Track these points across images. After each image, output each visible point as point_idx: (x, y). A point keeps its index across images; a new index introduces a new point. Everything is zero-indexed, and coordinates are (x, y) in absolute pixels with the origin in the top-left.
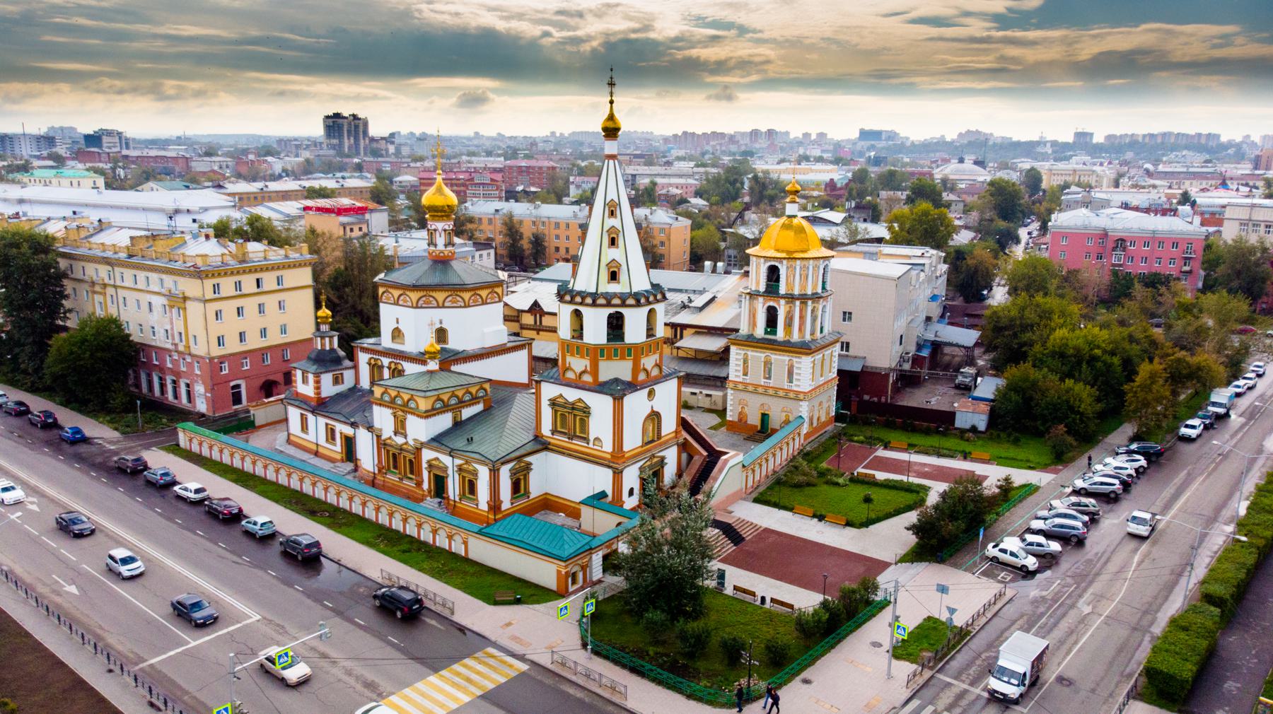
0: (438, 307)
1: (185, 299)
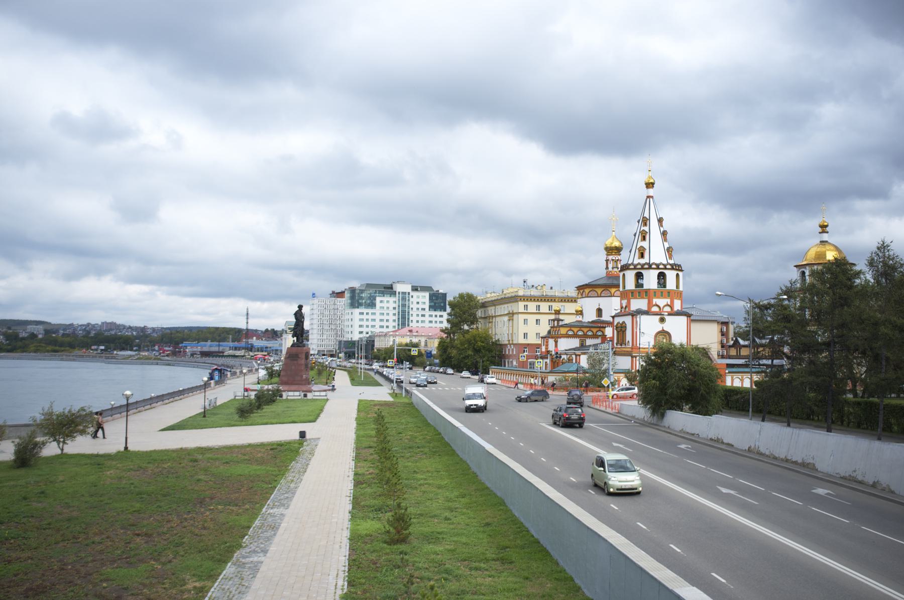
1: (513, 314)
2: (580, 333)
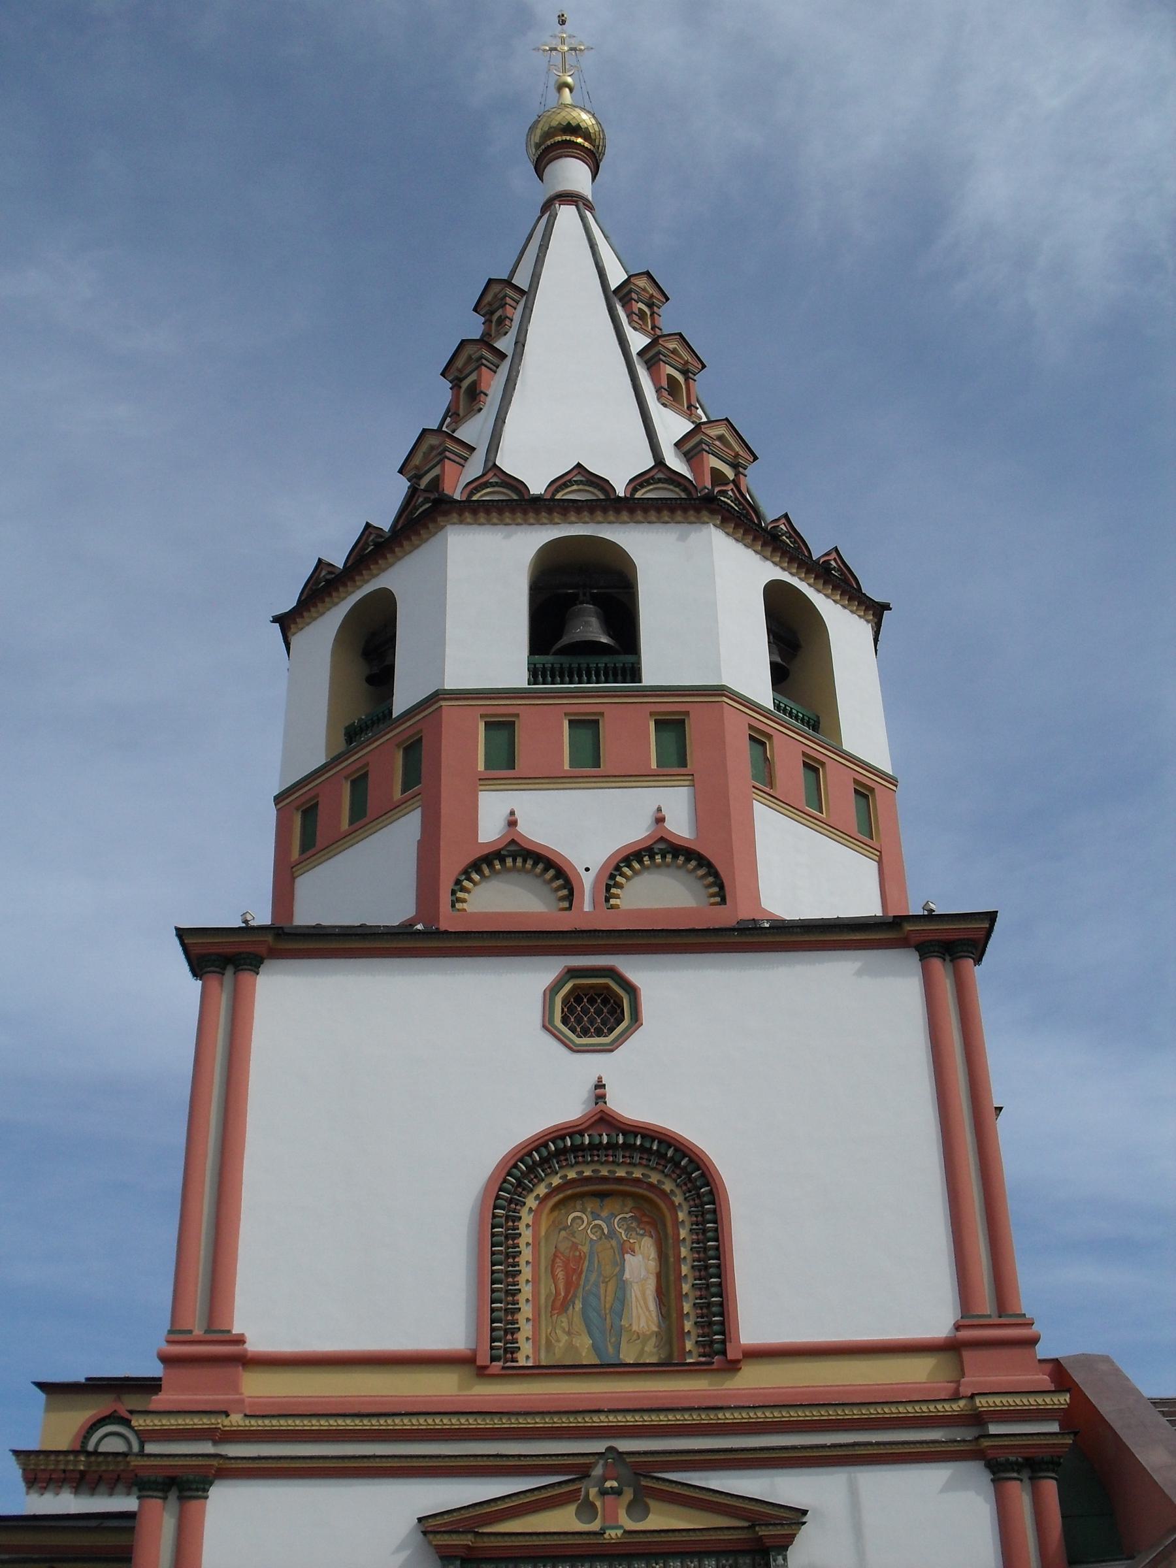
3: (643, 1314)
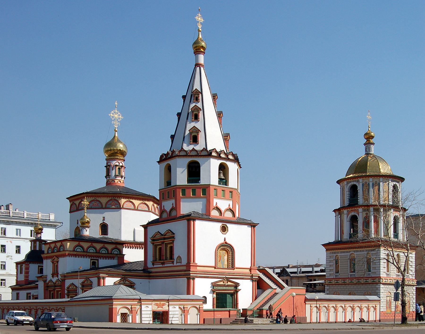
0: (102, 208)
2: (92, 250)
3: (226, 263)
